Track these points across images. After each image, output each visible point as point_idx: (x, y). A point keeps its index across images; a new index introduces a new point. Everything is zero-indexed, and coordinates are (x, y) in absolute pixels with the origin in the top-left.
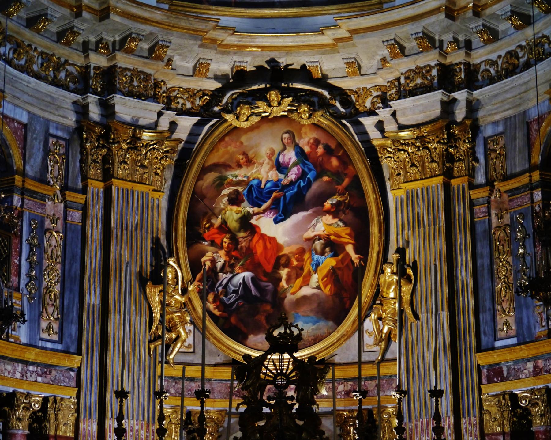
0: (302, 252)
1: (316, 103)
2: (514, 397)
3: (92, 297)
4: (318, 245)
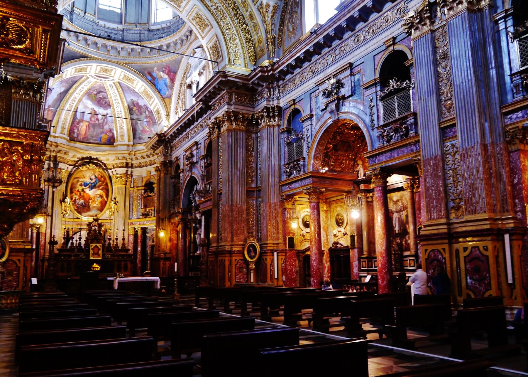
1: (100, 166)
2: (135, 228)
4: (98, 196)
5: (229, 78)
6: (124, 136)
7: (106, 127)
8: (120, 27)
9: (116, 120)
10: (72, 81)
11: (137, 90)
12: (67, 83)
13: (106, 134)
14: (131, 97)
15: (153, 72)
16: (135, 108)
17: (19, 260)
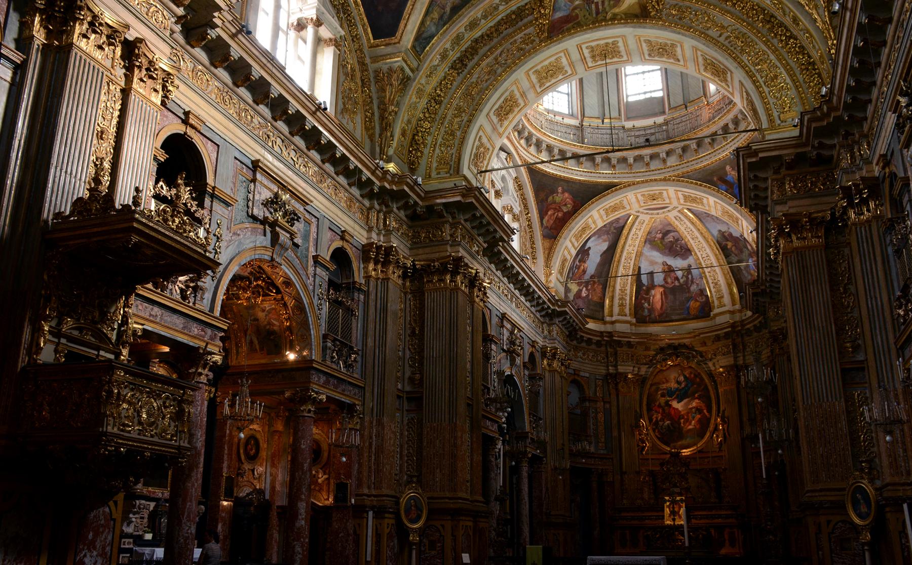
0: (688, 413)
3: (615, 434)
5: (761, 155)
6: (722, 297)
7: (694, 288)
8: (660, 120)
9: (704, 273)
10: (615, 228)
11: (713, 213)
12: (608, 234)
13: (696, 301)
14: (715, 229)
15: (726, 174)
16: (730, 245)
17: (443, 526)
